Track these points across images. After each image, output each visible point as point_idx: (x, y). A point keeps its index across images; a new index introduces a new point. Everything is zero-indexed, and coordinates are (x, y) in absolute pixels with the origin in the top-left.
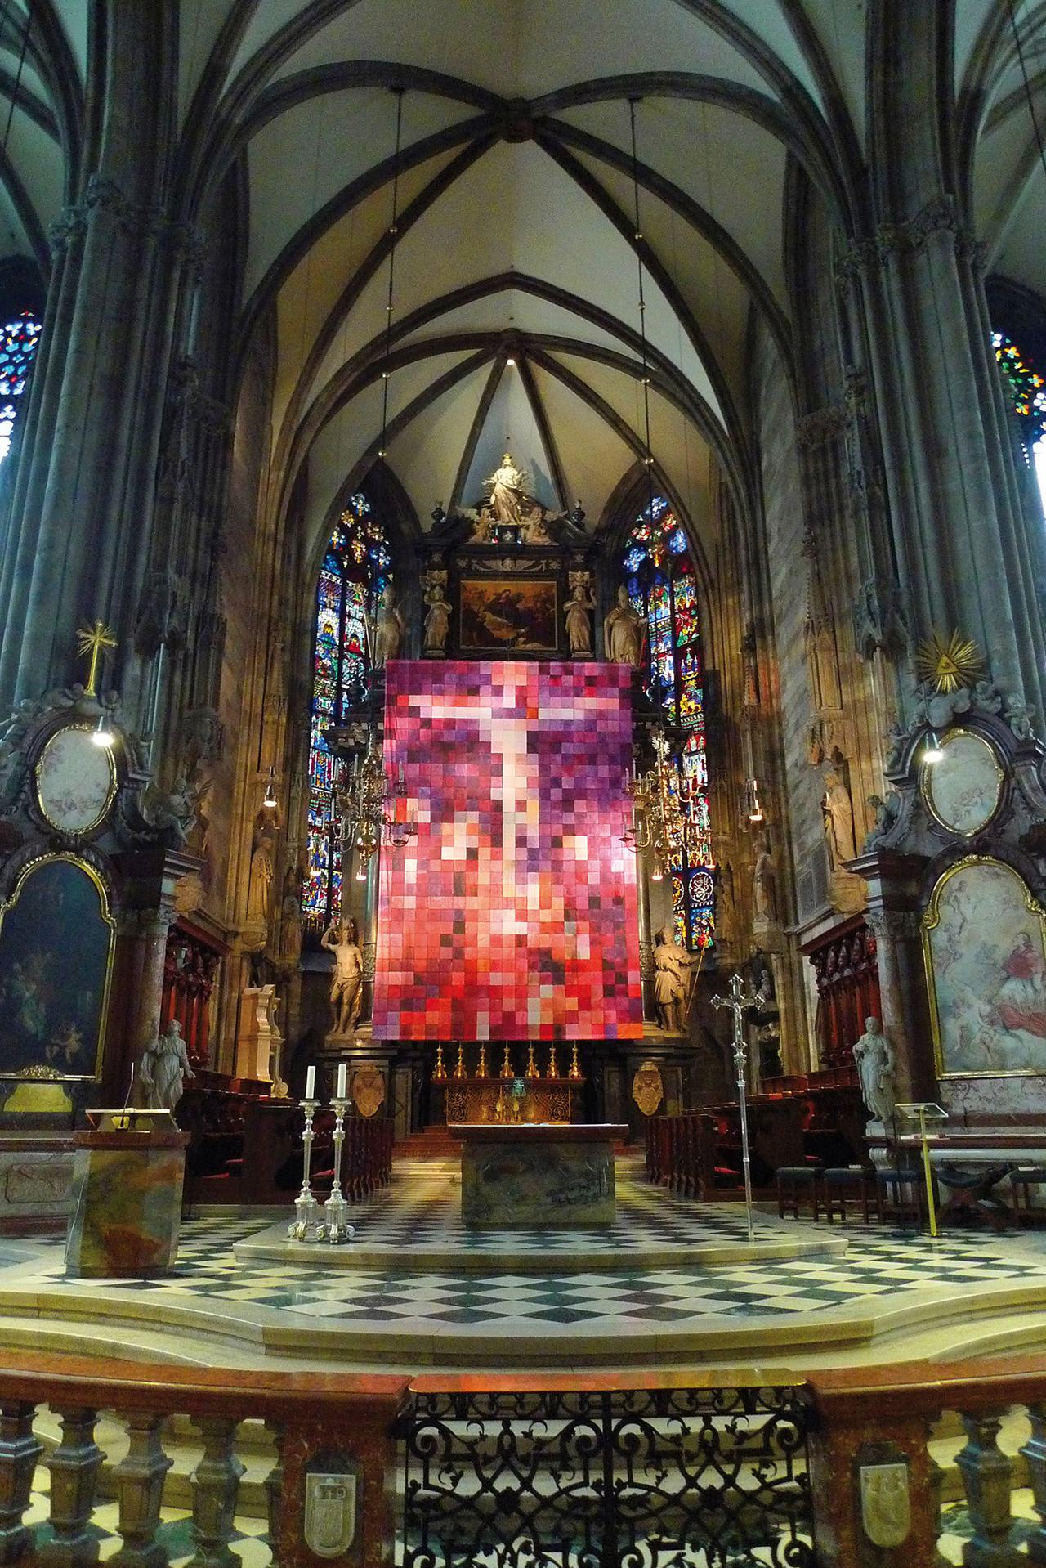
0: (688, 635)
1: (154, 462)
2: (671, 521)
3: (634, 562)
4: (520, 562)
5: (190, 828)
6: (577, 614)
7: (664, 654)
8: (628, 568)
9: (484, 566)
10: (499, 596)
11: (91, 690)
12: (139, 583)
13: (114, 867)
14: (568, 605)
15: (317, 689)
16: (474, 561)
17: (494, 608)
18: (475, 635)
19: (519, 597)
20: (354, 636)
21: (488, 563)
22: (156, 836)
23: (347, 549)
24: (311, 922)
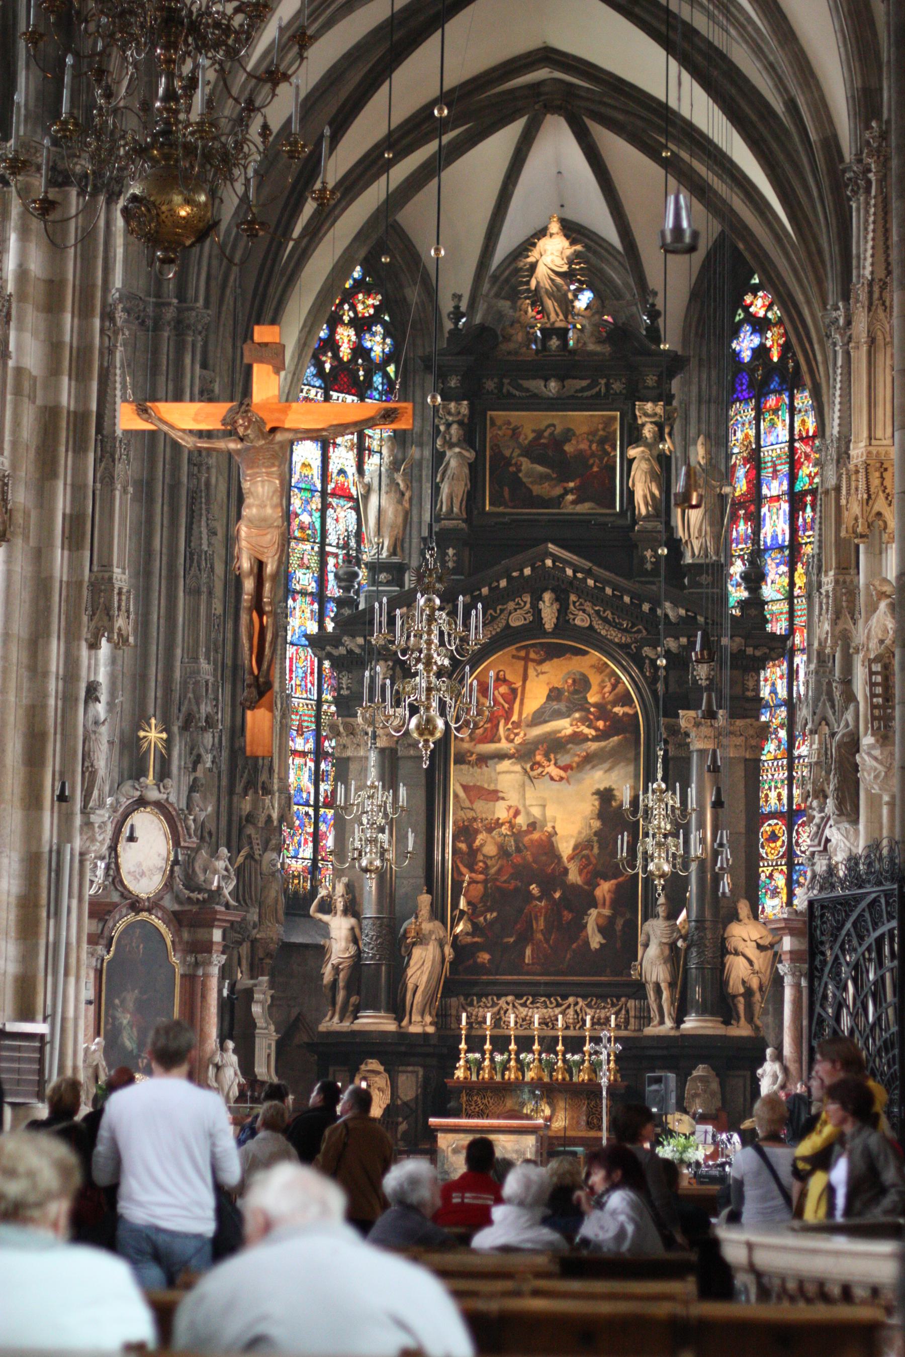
0: (809, 476)
1: (181, 560)
4: (568, 382)
5: (231, 887)
6: (644, 466)
7: (778, 498)
8: (736, 354)
9: (519, 388)
10: (539, 434)
11: (150, 780)
12: (177, 674)
13: (177, 920)
15: (294, 561)
16: (506, 381)
17: (534, 452)
19: (568, 435)
20: (342, 472)
21: (526, 384)
22: (206, 895)
24: (294, 877)
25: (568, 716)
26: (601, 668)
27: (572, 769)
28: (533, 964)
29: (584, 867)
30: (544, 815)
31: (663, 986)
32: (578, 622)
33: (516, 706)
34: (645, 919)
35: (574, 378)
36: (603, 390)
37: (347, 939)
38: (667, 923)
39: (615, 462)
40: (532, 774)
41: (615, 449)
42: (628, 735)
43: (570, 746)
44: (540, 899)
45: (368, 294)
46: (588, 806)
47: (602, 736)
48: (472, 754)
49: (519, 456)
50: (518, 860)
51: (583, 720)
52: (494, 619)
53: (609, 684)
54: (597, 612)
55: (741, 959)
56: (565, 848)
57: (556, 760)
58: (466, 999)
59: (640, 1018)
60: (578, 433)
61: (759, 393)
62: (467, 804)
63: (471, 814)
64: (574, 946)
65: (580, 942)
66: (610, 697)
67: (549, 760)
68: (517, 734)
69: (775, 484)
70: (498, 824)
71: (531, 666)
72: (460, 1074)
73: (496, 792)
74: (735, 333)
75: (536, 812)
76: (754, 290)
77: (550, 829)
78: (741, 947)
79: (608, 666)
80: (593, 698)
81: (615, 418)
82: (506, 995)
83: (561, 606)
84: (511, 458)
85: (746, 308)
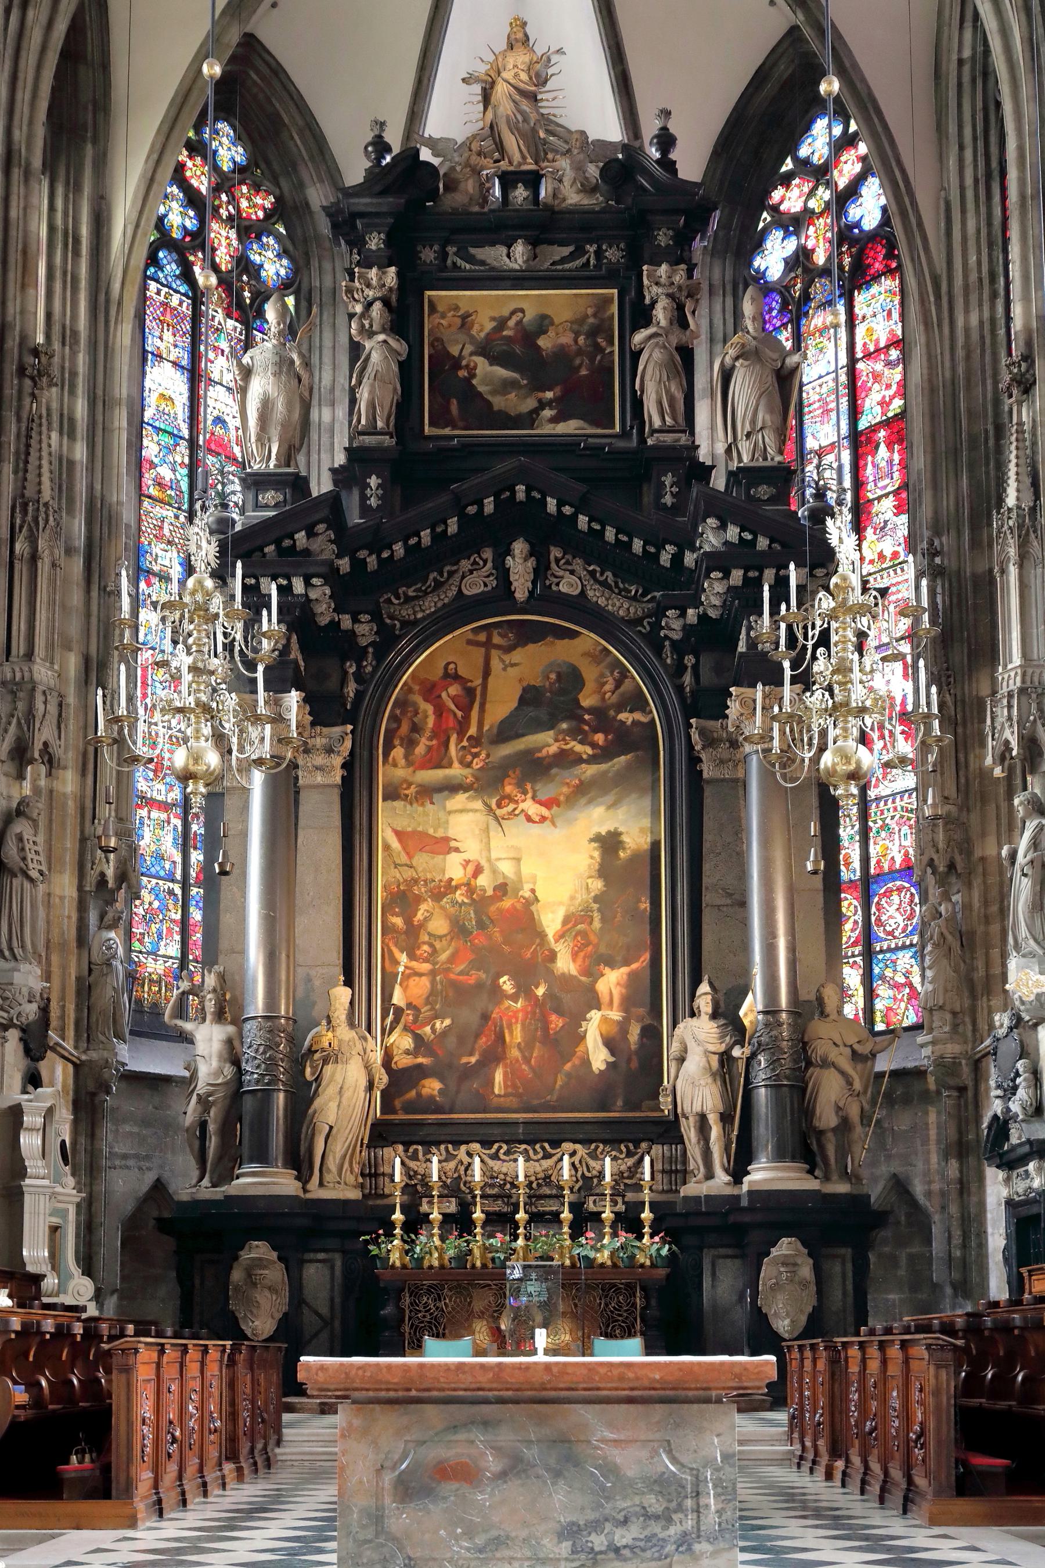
2: (848, 168)
14: (639, 337)
18: (454, 407)
23: (198, 239)
25: (551, 728)
27: (558, 805)
28: (505, 1095)
29: (580, 950)
30: (518, 873)
31: (713, 1119)
32: (564, 588)
33: (475, 714)
34: (675, 1024)
35: (551, 243)
36: (592, 262)
37: (220, 1057)
38: (713, 1024)
39: (613, 362)
40: (499, 812)
41: (612, 344)
42: (640, 753)
43: (554, 771)
44: (514, 998)
45: (257, 188)
47: (604, 755)
48: (410, 785)
49: (472, 354)
50: (480, 941)
52: (439, 585)
53: (610, 680)
54: (592, 573)
56: (551, 922)
57: (535, 792)
58: (406, 1151)
59: (671, 1172)
60: (557, 321)
62: (404, 859)
63: (409, 874)
64: (568, 1067)
65: (576, 1061)
66: (612, 699)
67: (525, 793)
68: (476, 755)
70: (450, 887)
71: (494, 653)
73: (447, 839)
75: (506, 868)
77: (527, 894)
79: (610, 652)
80: (587, 700)
81: (608, 300)
82: (467, 1143)
83: (538, 561)
84: (461, 357)
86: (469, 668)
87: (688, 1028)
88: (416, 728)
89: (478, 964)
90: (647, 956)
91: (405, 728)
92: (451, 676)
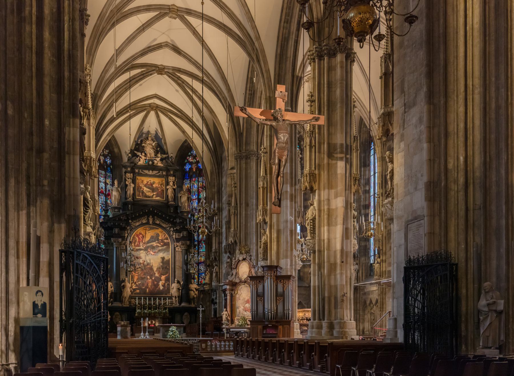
3: (187, 167)
6: (171, 190)
19: (154, 183)
26: (161, 232)
46: (160, 260)
47: (162, 246)
50: (145, 271)
51: (158, 243)
55: (192, 292)
56: (155, 269)
61: (191, 178)
69: (194, 196)
70: (141, 264)
71: (147, 231)
72: (137, 315)
73: (140, 257)
74: (185, 164)
75: (148, 261)
76: (189, 156)
77: (151, 265)
78: (193, 289)
80: (160, 238)
85: (187, 160)
86: (143, 232)
87: (174, 285)
88: (136, 241)
89: (145, 274)
90: (168, 274)
91: (134, 241)
92: (140, 234)
